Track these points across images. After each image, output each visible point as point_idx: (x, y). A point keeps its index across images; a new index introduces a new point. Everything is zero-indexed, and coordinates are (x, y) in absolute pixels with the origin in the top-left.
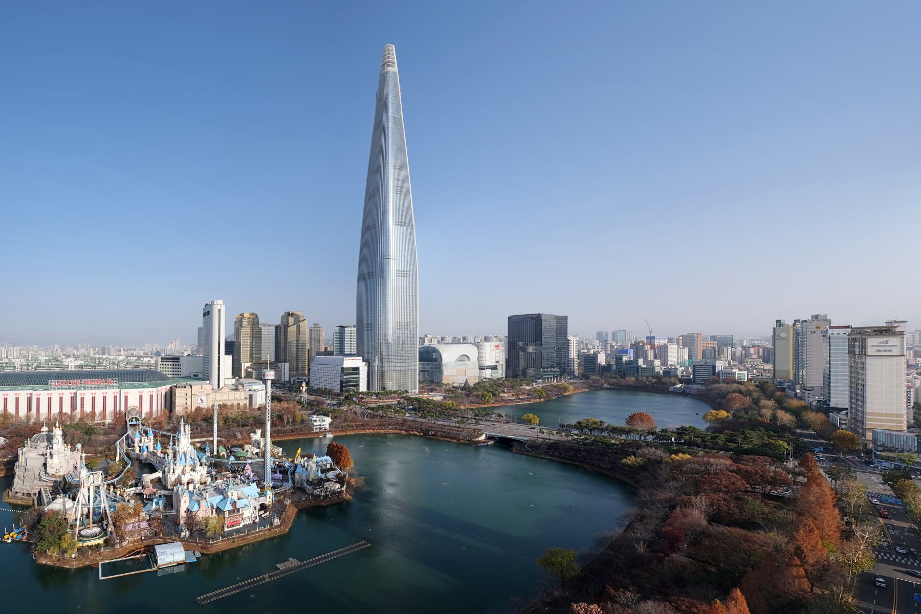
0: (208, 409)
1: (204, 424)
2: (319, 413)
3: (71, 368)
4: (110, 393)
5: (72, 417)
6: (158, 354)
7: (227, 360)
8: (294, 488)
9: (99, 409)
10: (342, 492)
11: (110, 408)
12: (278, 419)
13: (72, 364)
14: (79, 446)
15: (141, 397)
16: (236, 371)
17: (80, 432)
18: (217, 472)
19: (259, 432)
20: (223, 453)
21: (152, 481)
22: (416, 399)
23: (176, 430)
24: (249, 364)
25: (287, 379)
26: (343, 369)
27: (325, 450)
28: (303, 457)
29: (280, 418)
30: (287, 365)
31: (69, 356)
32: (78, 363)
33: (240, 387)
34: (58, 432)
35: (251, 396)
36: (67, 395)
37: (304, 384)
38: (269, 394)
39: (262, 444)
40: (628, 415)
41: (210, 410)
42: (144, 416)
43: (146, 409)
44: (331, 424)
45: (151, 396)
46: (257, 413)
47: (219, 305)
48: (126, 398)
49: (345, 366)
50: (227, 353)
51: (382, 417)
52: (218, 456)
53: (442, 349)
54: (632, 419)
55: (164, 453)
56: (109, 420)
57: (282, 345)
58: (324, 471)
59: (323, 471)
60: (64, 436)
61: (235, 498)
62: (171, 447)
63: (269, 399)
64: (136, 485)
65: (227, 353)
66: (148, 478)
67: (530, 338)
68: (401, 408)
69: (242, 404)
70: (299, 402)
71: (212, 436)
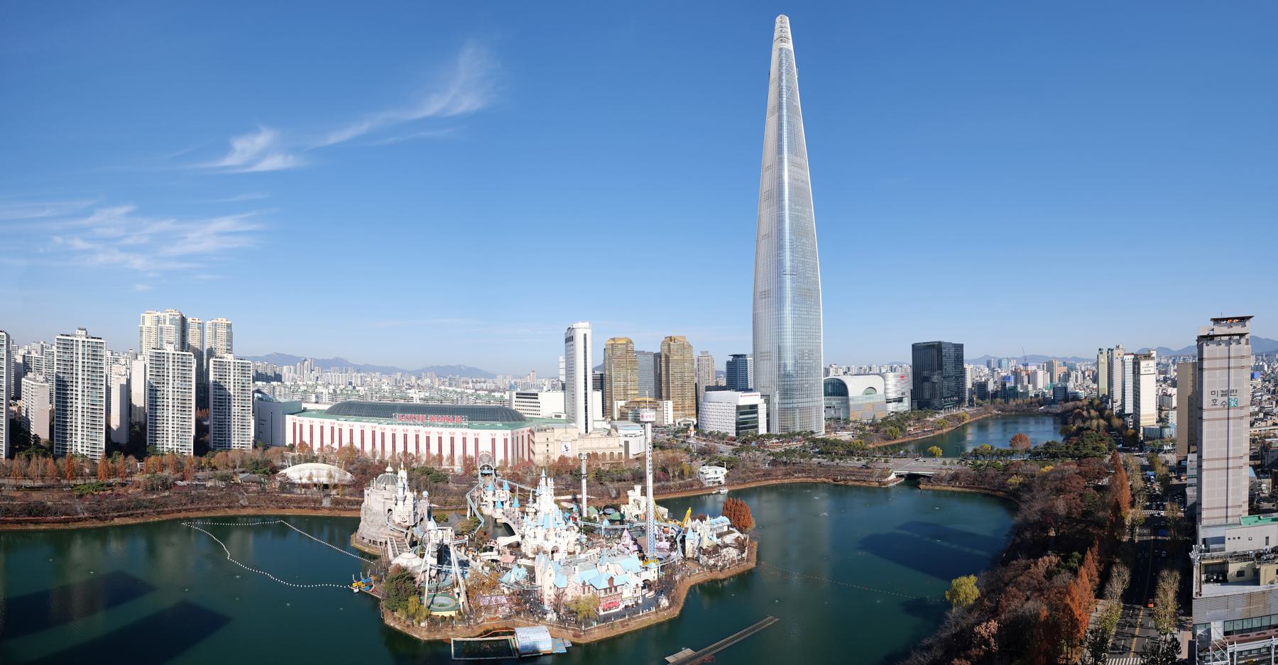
0: (575, 459)
1: (569, 478)
2: (709, 464)
3: (416, 401)
4: (458, 433)
5: (417, 459)
6: (512, 387)
7: (598, 395)
8: (685, 558)
9: (446, 452)
10: (742, 559)
11: (458, 452)
12: (662, 472)
13: (416, 397)
14: (425, 493)
15: (493, 440)
16: (606, 411)
17: (427, 478)
18: (589, 539)
19: (638, 488)
20: (594, 514)
21: (510, 546)
22: (825, 441)
23: (535, 484)
24: (622, 403)
25: (671, 422)
26: (738, 407)
27: (721, 506)
28: (693, 519)
29: (664, 470)
30: (670, 403)
31: (411, 387)
32: (422, 395)
33: (613, 432)
34: (403, 474)
35: (627, 443)
36: (412, 431)
37: (692, 428)
38: (650, 440)
39: (639, 502)
40: (1010, 436)
41: (577, 460)
42: (497, 464)
43: (500, 456)
44: (727, 476)
45: (506, 440)
46: (637, 465)
47: (582, 329)
48: (477, 440)
49: (741, 403)
50: (595, 389)
51: (785, 463)
52: (589, 519)
53: (847, 380)
54: (1014, 441)
55: (523, 512)
56: (458, 468)
57: (664, 378)
58: (720, 536)
59: (720, 536)
60: (410, 479)
61: (612, 573)
62: (530, 504)
63: (648, 449)
64: (491, 549)
65: (595, 389)
66: (503, 541)
67: (934, 369)
68: (804, 454)
69: (616, 453)
70: (687, 450)
71: (581, 493)
